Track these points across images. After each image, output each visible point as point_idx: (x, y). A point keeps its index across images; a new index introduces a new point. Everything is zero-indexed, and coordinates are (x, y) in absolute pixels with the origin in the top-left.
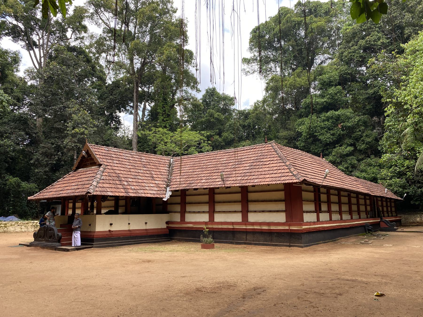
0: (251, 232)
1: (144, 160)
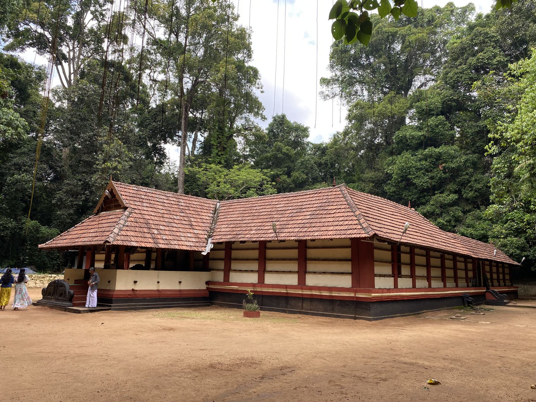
0: (307, 298)
1: (183, 204)
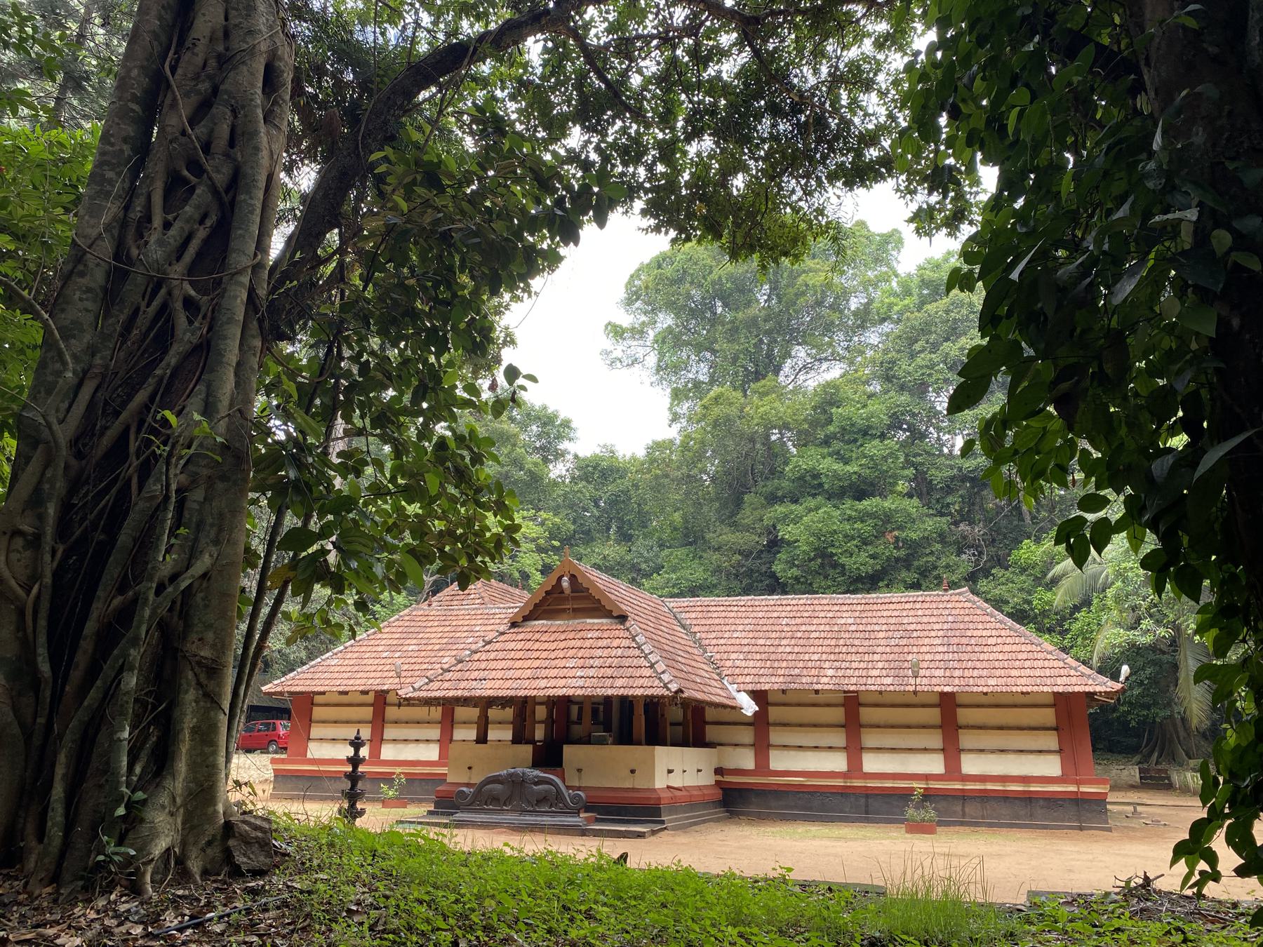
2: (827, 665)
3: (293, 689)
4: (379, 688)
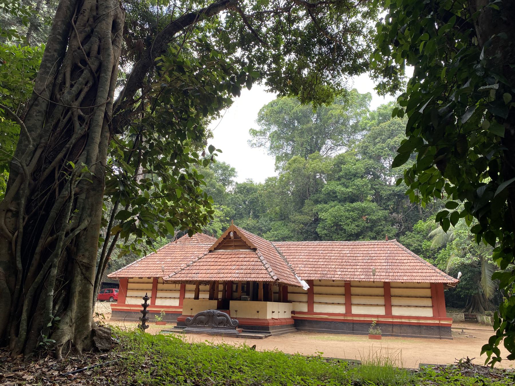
0: (397, 325)
2: (338, 270)
3: (120, 276)
4: (155, 276)
